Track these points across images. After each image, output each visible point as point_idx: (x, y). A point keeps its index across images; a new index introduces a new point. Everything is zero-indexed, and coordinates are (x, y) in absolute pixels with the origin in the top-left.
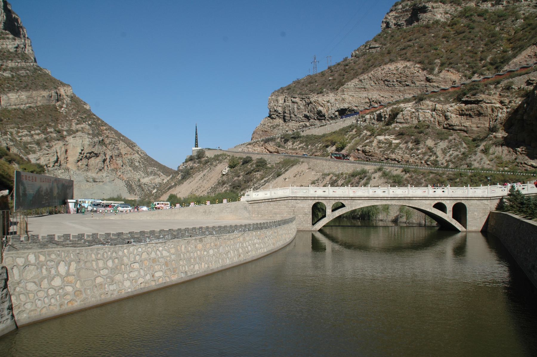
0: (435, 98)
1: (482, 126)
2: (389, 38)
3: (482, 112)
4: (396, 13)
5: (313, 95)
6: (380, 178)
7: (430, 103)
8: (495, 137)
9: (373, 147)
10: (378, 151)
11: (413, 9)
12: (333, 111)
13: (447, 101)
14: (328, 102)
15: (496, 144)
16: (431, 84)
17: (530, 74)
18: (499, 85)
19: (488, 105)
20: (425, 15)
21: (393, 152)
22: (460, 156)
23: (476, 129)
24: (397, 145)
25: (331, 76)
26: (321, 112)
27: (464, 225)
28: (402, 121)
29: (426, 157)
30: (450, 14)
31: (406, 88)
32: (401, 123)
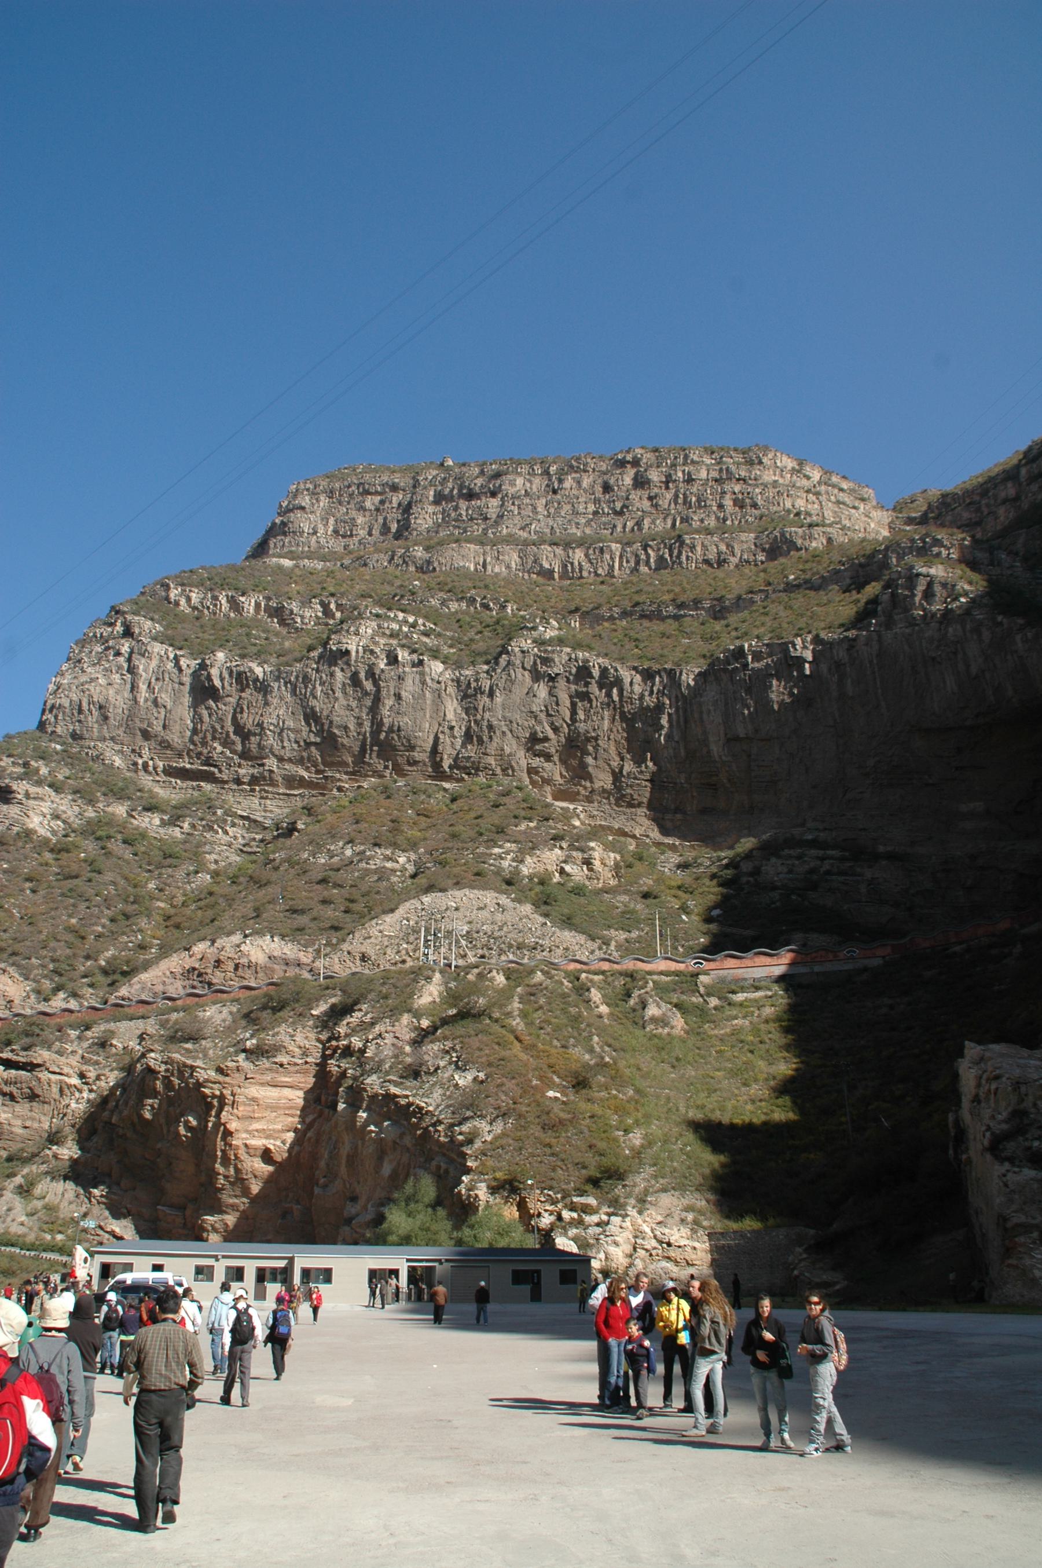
1: (36, 1125)
3: (38, 1091)
8: (55, 1156)
15: (53, 1175)
18: (89, 1034)
19: (53, 1077)
23: (20, 1131)
30: (64, 822)
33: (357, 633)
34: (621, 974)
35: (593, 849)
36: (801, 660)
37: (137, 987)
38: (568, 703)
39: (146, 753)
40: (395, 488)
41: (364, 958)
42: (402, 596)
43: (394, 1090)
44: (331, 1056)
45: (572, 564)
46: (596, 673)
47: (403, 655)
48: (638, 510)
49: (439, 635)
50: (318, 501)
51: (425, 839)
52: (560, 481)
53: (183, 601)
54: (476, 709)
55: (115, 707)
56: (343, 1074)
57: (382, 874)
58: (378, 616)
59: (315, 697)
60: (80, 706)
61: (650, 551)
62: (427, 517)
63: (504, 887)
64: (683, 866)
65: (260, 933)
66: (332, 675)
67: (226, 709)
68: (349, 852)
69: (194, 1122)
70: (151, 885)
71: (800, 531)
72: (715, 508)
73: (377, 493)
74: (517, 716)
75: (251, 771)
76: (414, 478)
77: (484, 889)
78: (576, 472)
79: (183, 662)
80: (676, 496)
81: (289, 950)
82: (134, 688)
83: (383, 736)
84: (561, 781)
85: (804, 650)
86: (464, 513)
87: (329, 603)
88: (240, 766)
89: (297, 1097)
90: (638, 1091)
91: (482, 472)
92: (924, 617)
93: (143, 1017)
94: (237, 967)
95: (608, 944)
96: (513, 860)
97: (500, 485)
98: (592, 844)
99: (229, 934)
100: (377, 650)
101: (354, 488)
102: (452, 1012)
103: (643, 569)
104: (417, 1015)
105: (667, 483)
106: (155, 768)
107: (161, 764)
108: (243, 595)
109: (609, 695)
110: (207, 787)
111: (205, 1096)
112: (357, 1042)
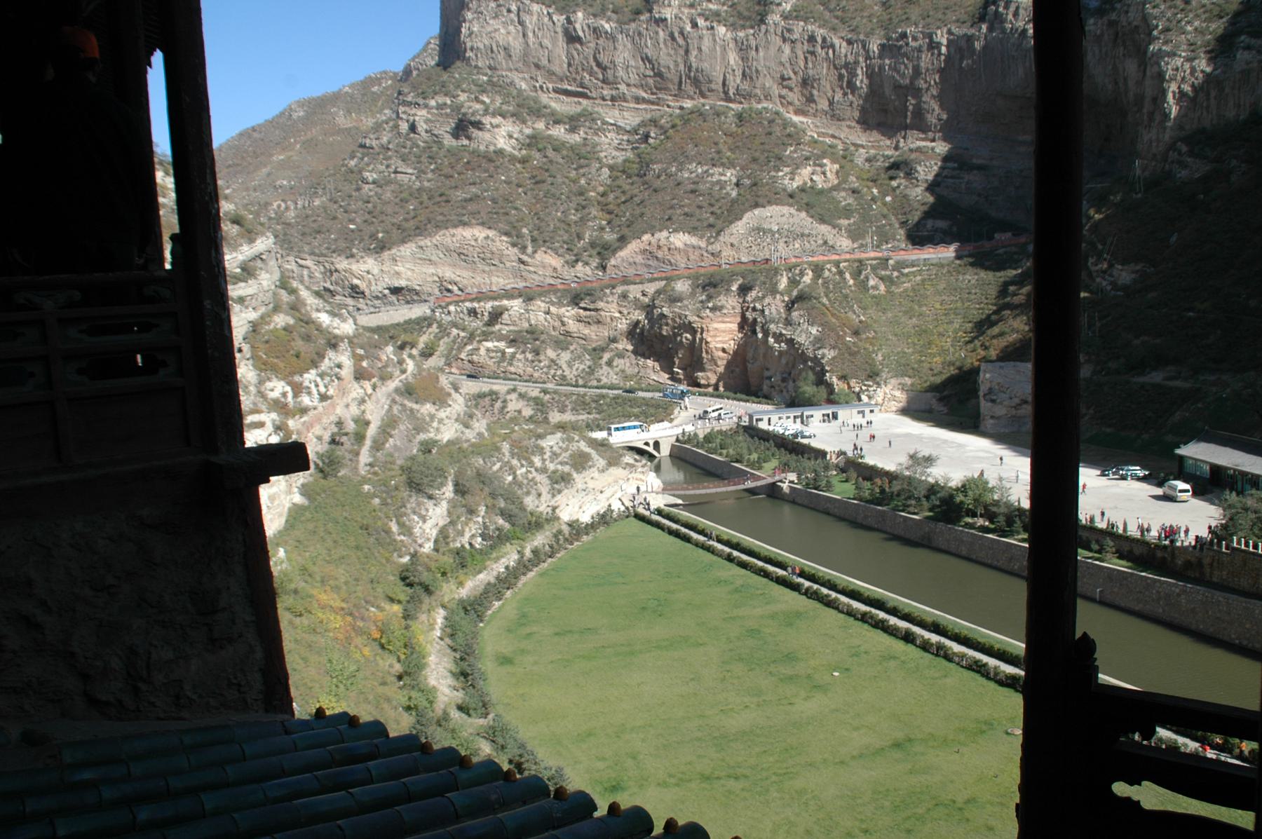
2: (424, 159)
5: (339, 258)
6: (517, 400)
7: (543, 305)
9: (482, 356)
10: (490, 363)
11: (461, 121)
12: (379, 287)
13: (560, 304)
14: (368, 272)
15: (621, 355)
17: (646, 285)
18: (614, 291)
20: (480, 133)
21: (511, 365)
24: (513, 356)
25: (352, 221)
26: (357, 286)
28: (509, 322)
29: (552, 372)
30: (517, 139)
31: (492, 267)
32: (507, 325)
33: (669, 5)
34: (855, 261)
35: (825, 165)
36: (939, 45)
37: (619, 260)
38: (802, 57)
41: (732, 245)
43: (784, 332)
46: (819, 40)
47: (701, 22)
54: (748, 59)
56: (755, 320)
63: (791, 200)
64: (868, 160)
65: (675, 231)
66: (657, 33)
67: (589, 50)
68: (700, 170)
69: (689, 336)
70: (583, 182)
74: (772, 65)
79: (555, 18)
81: (693, 240)
82: (524, 35)
83: (692, 74)
85: (942, 37)
89: (735, 327)
92: (1012, 29)
93: (641, 283)
94: (669, 249)
95: (841, 230)
98: (825, 161)
99: (661, 231)
100: (684, 17)
102: (795, 293)
107: (550, 86)
109: (827, 54)
110: (584, 102)
112: (758, 306)
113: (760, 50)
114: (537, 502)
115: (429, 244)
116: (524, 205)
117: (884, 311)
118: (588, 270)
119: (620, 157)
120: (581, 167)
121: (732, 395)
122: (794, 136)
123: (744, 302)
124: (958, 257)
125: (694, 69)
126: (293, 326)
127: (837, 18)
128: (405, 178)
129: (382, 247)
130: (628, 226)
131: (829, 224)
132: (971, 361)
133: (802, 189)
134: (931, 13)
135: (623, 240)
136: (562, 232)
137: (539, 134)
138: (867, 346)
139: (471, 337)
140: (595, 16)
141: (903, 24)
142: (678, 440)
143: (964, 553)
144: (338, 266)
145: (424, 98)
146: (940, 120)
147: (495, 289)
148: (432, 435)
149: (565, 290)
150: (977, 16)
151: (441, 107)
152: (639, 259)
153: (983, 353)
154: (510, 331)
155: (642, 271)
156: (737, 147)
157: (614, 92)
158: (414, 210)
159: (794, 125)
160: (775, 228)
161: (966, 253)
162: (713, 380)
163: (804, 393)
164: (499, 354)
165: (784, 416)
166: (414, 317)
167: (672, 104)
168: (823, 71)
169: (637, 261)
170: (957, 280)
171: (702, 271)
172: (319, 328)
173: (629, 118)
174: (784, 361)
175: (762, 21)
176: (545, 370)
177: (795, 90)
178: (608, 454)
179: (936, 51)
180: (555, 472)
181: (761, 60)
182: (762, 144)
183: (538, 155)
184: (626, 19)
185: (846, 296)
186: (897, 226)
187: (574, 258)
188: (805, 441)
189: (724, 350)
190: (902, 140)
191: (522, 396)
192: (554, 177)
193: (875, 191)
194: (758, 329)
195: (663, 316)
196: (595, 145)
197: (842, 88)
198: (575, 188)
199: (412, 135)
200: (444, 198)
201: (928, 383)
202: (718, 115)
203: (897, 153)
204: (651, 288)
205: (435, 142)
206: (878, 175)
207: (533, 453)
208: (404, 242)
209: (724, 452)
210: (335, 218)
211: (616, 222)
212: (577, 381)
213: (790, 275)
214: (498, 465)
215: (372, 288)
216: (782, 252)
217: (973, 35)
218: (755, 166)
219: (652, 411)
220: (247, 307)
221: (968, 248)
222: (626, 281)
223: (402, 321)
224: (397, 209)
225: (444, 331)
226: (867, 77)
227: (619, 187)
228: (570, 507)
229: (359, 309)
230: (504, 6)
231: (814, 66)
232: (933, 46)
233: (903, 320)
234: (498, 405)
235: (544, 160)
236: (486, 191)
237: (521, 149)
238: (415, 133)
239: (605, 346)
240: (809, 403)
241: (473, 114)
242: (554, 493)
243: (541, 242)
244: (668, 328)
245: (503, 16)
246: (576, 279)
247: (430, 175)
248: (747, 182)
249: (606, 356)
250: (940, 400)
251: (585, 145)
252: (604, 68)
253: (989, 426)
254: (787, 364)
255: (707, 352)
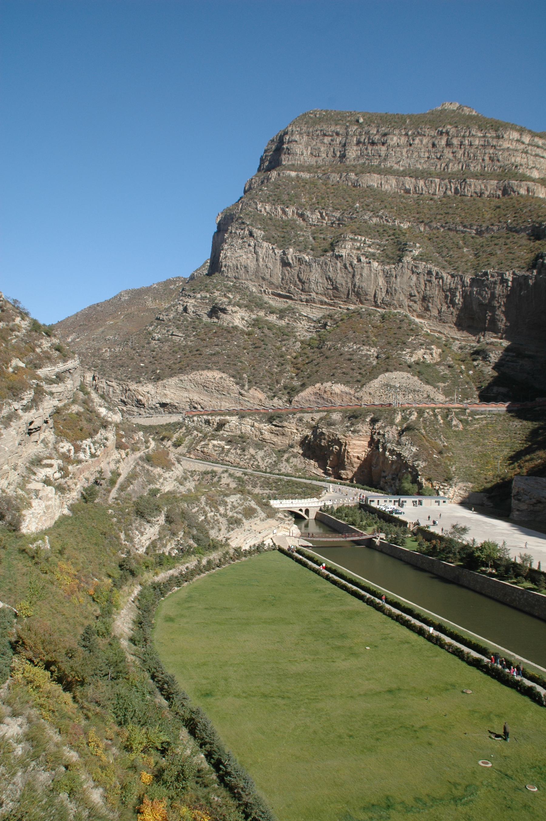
0: (252, 416)
4: (195, 301)
5: (132, 383)
6: (228, 477)
7: (250, 421)
10: (214, 453)
11: (214, 307)
12: (154, 402)
13: (261, 422)
14: (148, 393)
15: (295, 456)
16: (243, 398)
18: (295, 416)
20: (225, 316)
21: (227, 456)
22: (273, 463)
24: (229, 450)
25: (142, 361)
26: (140, 400)
27: (308, 517)
28: (229, 430)
29: (252, 462)
30: (246, 321)
31: (223, 396)
32: (227, 431)
35: (433, 349)
36: (507, 280)
37: (300, 397)
38: (423, 283)
39: (264, 286)
40: (338, 134)
41: (370, 394)
42: (353, 214)
43: (396, 449)
44: (374, 434)
45: (419, 187)
46: (434, 273)
47: (363, 259)
48: (447, 158)
49: (373, 243)
50: (303, 138)
51: (379, 342)
52: (413, 140)
53: (263, 210)
54: (390, 282)
55: (251, 268)
56: (379, 440)
57: (368, 357)
58: (351, 239)
59: (330, 272)
60: (237, 266)
61: (452, 185)
62: (353, 152)
63: (409, 369)
64: (461, 348)
65: (336, 382)
66: (336, 264)
67: (295, 272)
68: (355, 347)
69: (337, 447)
70: (284, 349)
71: (516, 183)
72: (481, 161)
73: (329, 136)
74: (405, 287)
75: (306, 297)
76: (346, 129)
77: (404, 371)
78: (420, 135)
79: (276, 251)
80: (464, 153)
81: (347, 389)
83: (356, 289)
84: (420, 311)
85: (509, 276)
86: (370, 152)
87: (323, 213)
88: (301, 294)
89: (366, 444)
90: (453, 453)
91: (378, 131)
93: (312, 413)
94: (331, 393)
96: (410, 356)
97: (386, 140)
98: (433, 347)
99: (327, 382)
100: (353, 256)
101: (318, 132)
102: (405, 426)
103: (449, 193)
104: (397, 426)
105: (461, 145)
106: (268, 293)
107: (270, 291)
108: (287, 207)
109: (439, 282)
110: (290, 302)
111: (341, 442)
113: (398, 277)
114: (217, 534)
115: (186, 379)
116: (246, 360)
117: (460, 441)
118: (280, 403)
119: (308, 336)
120: (284, 340)
121: (361, 486)
122: (415, 330)
123: (373, 429)
124: (509, 410)
125: (357, 287)
126: (82, 413)
127: (446, 261)
128: (177, 339)
129: (158, 378)
130: (308, 378)
131: (432, 385)
132: (511, 474)
133: (417, 363)
134: (503, 261)
135: (304, 386)
136: (267, 378)
137: (260, 318)
138: (447, 461)
139: (205, 437)
140: (300, 251)
141: (486, 267)
142: (321, 510)
143: (478, 589)
144: (130, 387)
145: (194, 293)
146: (506, 326)
147: (223, 409)
148: (158, 486)
149: (265, 413)
150: (531, 264)
151: (203, 298)
152: (312, 398)
153: (518, 470)
154: (229, 435)
155: (314, 405)
156: (380, 335)
157: (308, 297)
158: (180, 358)
159: (416, 324)
160: (398, 385)
161: (515, 408)
162: (350, 475)
163: (404, 487)
164: (220, 449)
165: (388, 500)
166: (172, 422)
167: (343, 306)
168: (436, 293)
169: (311, 399)
170: (509, 425)
171: (350, 408)
172: (98, 415)
173: (316, 313)
174: (394, 467)
175: (400, 261)
176: (247, 461)
177: (418, 303)
178: (268, 511)
179: (505, 284)
180: (232, 517)
181: (398, 283)
182: (395, 334)
183: (258, 331)
184: (319, 255)
185: (437, 430)
186: (475, 389)
187: (273, 394)
188: (396, 516)
189: (358, 458)
190: (482, 337)
191: (231, 475)
192: (267, 345)
193: (463, 367)
194: (380, 446)
195: (322, 434)
196: (294, 328)
197: (447, 303)
198: (278, 352)
199: (184, 314)
200: (198, 352)
201: (483, 487)
202: (370, 315)
203: (479, 345)
204: (317, 416)
205: (198, 319)
206: (466, 357)
207: (220, 505)
208: (171, 376)
209: (346, 518)
210: (133, 359)
211: (301, 374)
212: (266, 469)
213: (403, 414)
214: (196, 509)
215: (150, 402)
216: (400, 400)
217: (528, 276)
218: (389, 347)
219: (310, 491)
220: (54, 398)
221: (517, 406)
222: (302, 410)
223: (165, 424)
224: (170, 357)
225: (189, 431)
226: (462, 298)
227: (305, 354)
228: (238, 540)
229: (140, 414)
230: (247, 242)
231: (430, 289)
232: (504, 281)
233: (472, 447)
234: (216, 479)
235: (262, 334)
236: (224, 350)
237: (248, 327)
238: (186, 313)
239: (286, 449)
240: (406, 493)
241: (221, 304)
242: (229, 529)
243: (254, 384)
244: (325, 441)
245: (246, 248)
246: (273, 407)
247: (192, 338)
248: (383, 356)
249: (286, 456)
250: (489, 498)
251: (288, 327)
252: (303, 283)
253: (515, 516)
254: (396, 469)
255: (348, 458)
